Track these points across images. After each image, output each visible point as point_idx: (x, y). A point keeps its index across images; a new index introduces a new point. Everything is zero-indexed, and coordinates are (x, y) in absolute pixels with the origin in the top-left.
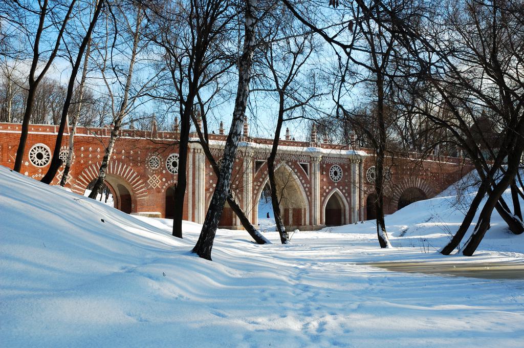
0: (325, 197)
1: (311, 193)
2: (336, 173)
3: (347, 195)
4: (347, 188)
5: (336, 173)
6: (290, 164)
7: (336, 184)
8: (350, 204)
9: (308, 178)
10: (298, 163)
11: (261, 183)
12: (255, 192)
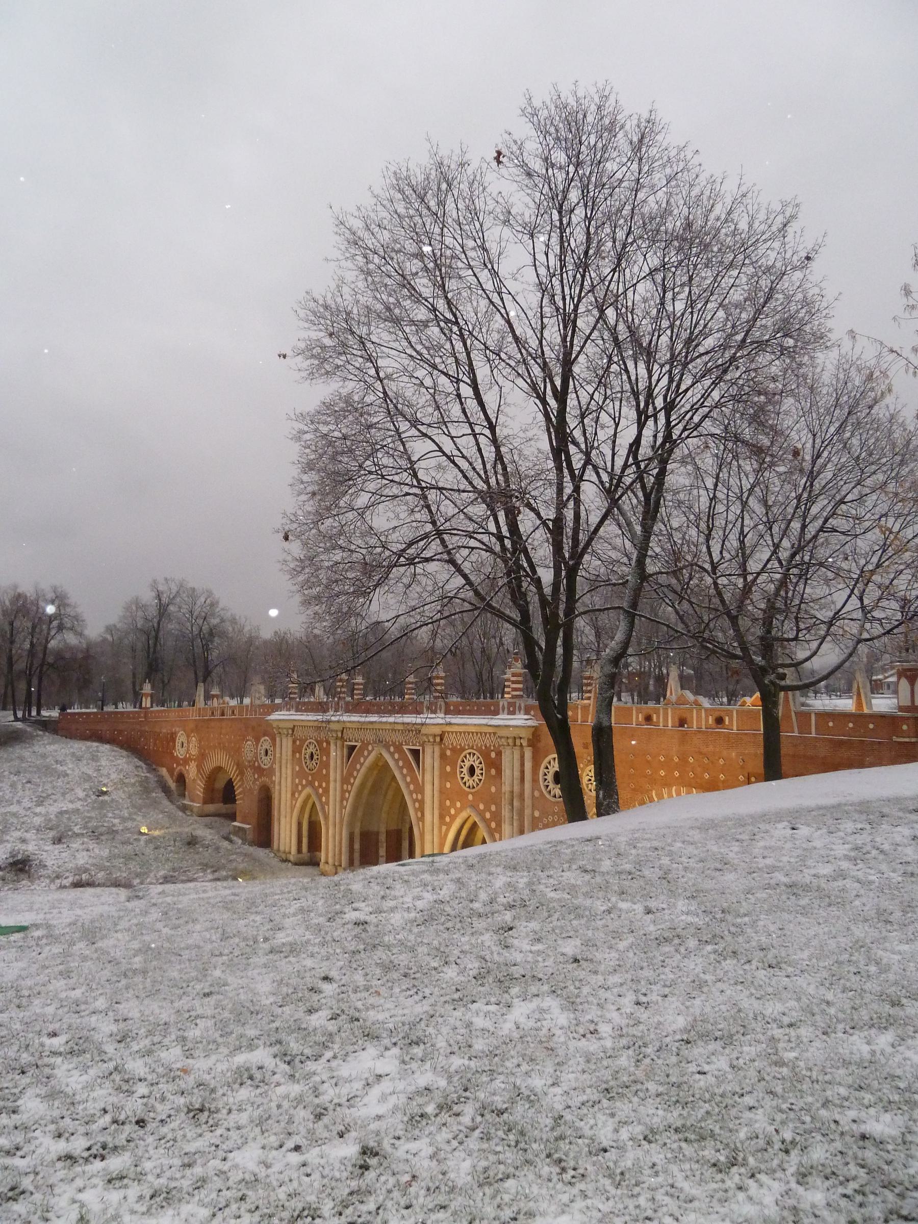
0: (449, 826)
1: (423, 815)
2: (472, 771)
3: (493, 825)
5: (472, 771)
6: (392, 749)
7: (470, 797)
9: (420, 778)
10: (405, 747)
11: (352, 785)
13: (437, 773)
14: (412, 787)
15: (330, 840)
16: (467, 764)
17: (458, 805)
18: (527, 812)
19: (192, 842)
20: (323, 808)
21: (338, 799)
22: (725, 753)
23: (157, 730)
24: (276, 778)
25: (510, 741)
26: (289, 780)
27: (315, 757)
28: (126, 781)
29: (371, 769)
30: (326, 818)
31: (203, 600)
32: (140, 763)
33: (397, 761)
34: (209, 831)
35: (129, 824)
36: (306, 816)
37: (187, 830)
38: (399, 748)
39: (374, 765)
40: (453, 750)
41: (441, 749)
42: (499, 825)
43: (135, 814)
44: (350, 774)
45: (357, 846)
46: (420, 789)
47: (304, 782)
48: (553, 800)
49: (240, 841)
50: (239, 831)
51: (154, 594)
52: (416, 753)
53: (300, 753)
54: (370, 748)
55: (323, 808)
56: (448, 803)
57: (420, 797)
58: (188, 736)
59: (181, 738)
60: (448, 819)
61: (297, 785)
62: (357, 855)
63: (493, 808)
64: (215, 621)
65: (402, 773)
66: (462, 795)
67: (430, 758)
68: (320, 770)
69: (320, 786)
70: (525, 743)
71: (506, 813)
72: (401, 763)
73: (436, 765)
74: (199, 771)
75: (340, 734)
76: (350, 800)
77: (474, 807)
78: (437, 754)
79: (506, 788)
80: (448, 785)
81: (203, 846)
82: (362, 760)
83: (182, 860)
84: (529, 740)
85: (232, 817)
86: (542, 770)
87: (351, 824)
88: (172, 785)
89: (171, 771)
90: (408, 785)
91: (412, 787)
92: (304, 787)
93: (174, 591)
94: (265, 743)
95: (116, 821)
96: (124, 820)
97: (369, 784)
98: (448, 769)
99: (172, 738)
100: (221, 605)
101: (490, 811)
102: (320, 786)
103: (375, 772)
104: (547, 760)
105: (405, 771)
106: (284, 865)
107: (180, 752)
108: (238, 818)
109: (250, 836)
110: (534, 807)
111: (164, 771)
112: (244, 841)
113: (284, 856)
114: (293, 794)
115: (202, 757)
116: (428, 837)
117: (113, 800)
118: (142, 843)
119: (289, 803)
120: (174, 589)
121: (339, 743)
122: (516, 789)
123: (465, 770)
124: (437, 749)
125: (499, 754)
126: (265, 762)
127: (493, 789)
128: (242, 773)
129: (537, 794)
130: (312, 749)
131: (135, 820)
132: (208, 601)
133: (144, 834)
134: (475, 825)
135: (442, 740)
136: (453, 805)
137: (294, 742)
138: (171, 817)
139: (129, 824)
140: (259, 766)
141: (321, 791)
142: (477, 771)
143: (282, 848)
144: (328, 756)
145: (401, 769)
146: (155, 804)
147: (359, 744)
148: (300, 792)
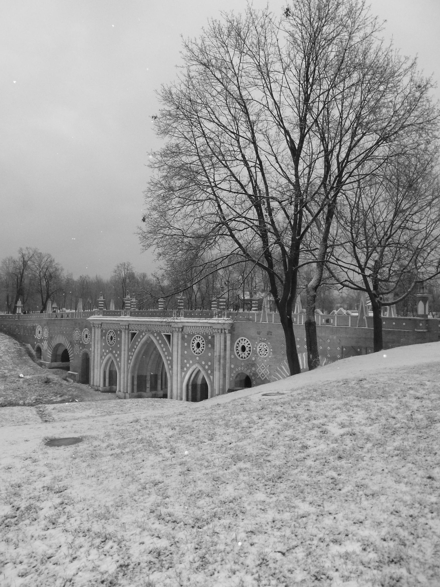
0: (186, 373)
1: (172, 367)
2: (198, 345)
3: (209, 372)
4: (209, 363)
5: (198, 345)
6: (155, 335)
7: (197, 358)
8: (212, 383)
9: (171, 349)
10: (162, 334)
11: (134, 352)
12: (130, 361)
13: (180, 346)
14: (166, 353)
15: (122, 380)
16: (196, 342)
17: (191, 362)
18: (228, 365)
19: (47, 382)
20: (118, 364)
21: (126, 360)
22: (331, 337)
23: (25, 324)
24: (92, 349)
25: (220, 331)
26: (99, 350)
27: (114, 338)
28: (9, 351)
29: (143, 345)
30: (120, 369)
31: (46, 259)
32: (16, 342)
33: (158, 341)
34: (55, 376)
35: (13, 373)
36: (108, 368)
37: (44, 375)
38: (159, 334)
39: (146, 342)
40: (189, 335)
41: (182, 334)
42: (212, 372)
43: (16, 367)
44: (133, 347)
45: (136, 383)
46: (170, 354)
47: (107, 351)
48: (241, 359)
49: (72, 381)
50: (71, 376)
51: (20, 255)
52: (168, 337)
53: (105, 336)
54: (144, 334)
55: (118, 364)
56: (185, 361)
57: (170, 358)
58: (43, 328)
59: (39, 328)
60: (185, 369)
61: (104, 353)
62: (135, 387)
63: (209, 363)
64: (51, 270)
65: (161, 347)
66: (193, 357)
67: (176, 339)
68: (116, 345)
69: (116, 353)
70: (227, 331)
71: (216, 366)
72: (160, 342)
73: (180, 342)
74: (49, 346)
75: (127, 327)
76: (133, 360)
77: (199, 363)
78: (180, 337)
79: (217, 354)
80: (186, 352)
81: (53, 383)
82: (139, 340)
83: (43, 390)
84: (229, 330)
85: (68, 369)
86: (236, 344)
87: (133, 372)
88: (34, 352)
89: (33, 346)
90: (164, 352)
91: (166, 353)
92: (107, 354)
93: (31, 254)
94: (86, 331)
95: (6, 371)
96: (10, 370)
97: (142, 352)
98: (186, 344)
99: (34, 328)
100: (56, 262)
101: (208, 365)
102: (116, 353)
103: (146, 346)
104: (238, 340)
105: (162, 345)
106: (97, 392)
107: (38, 336)
108: (71, 369)
109: (77, 378)
110: (231, 363)
111: (29, 346)
112: (75, 380)
113: (96, 388)
114: (101, 357)
115: (50, 339)
116: (175, 378)
117: (3, 361)
118: (21, 382)
119: (99, 361)
120: (31, 253)
121: (127, 331)
122: (222, 354)
123: (195, 345)
124: (180, 335)
125: (213, 337)
126: (86, 341)
127: (210, 354)
128: (73, 346)
129: (233, 356)
130: (111, 334)
131: (15, 370)
132: (49, 260)
133: (22, 378)
134: (199, 371)
135: (182, 330)
136: (188, 362)
137: (102, 331)
138: (34, 368)
139: (13, 373)
140: (82, 343)
141: (116, 355)
142: (201, 346)
143: (95, 384)
144: (121, 338)
145: (160, 344)
146: (25, 362)
147: (137, 332)
148: (105, 356)
